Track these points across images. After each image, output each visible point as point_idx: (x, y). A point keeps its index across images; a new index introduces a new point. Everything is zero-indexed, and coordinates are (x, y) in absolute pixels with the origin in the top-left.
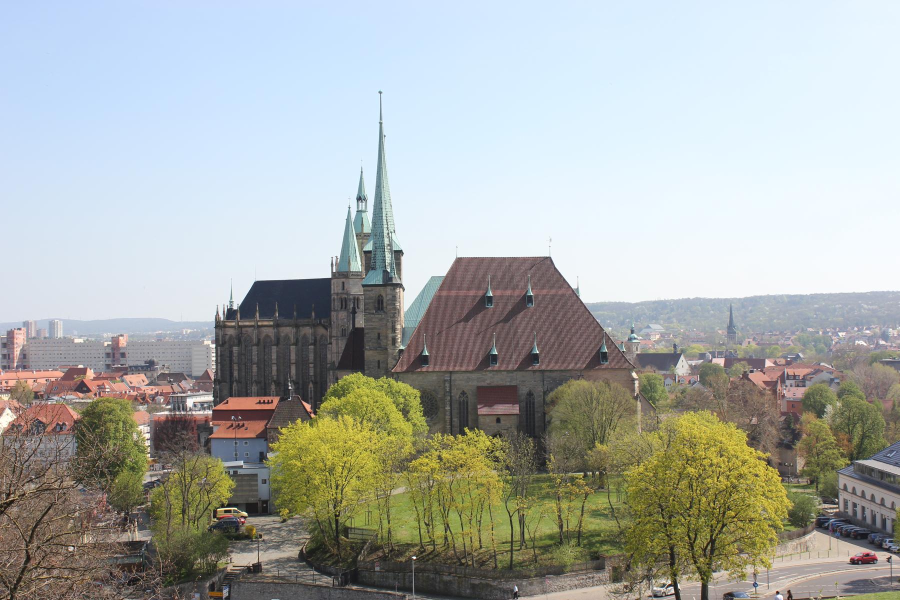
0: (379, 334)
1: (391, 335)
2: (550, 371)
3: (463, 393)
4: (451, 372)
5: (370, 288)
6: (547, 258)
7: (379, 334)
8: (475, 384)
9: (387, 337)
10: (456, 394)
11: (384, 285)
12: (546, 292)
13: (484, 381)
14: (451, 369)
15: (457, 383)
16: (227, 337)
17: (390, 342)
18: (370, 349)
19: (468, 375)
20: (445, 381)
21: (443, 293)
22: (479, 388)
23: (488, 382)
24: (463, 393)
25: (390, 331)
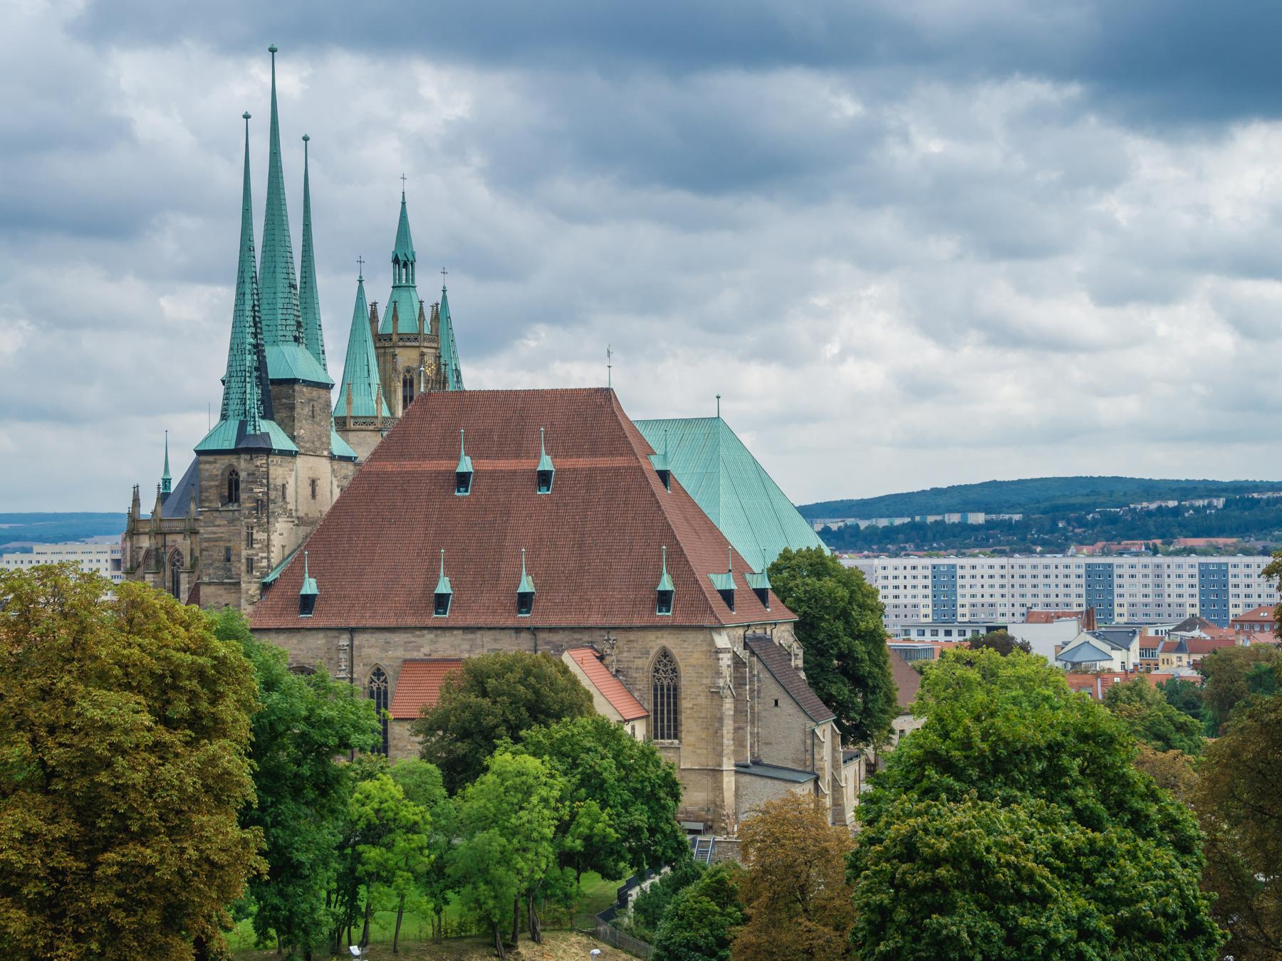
0: (228, 549)
1: (244, 553)
2: (551, 630)
3: (378, 673)
4: (352, 631)
5: (211, 458)
6: (602, 390)
7: (228, 549)
8: (401, 653)
9: (239, 555)
10: (362, 674)
11: (235, 452)
12: (582, 463)
13: (418, 648)
14: (353, 624)
15: (365, 651)
16: (142, 553)
17: (243, 568)
18: (209, 584)
19: (388, 636)
20: (339, 649)
21: (377, 466)
22: (406, 661)
23: (426, 650)
24: (378, 673)
25: (243, 544)
